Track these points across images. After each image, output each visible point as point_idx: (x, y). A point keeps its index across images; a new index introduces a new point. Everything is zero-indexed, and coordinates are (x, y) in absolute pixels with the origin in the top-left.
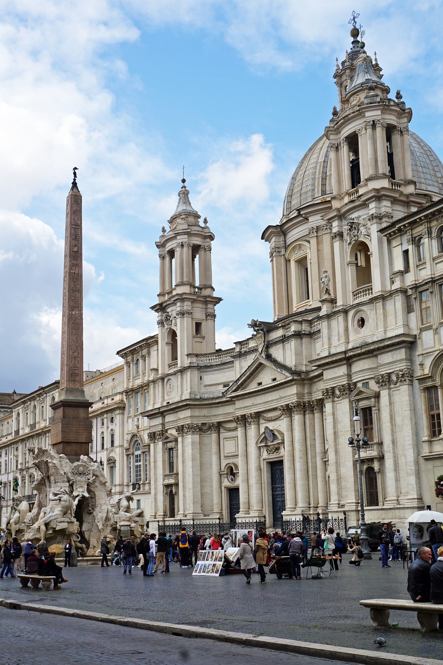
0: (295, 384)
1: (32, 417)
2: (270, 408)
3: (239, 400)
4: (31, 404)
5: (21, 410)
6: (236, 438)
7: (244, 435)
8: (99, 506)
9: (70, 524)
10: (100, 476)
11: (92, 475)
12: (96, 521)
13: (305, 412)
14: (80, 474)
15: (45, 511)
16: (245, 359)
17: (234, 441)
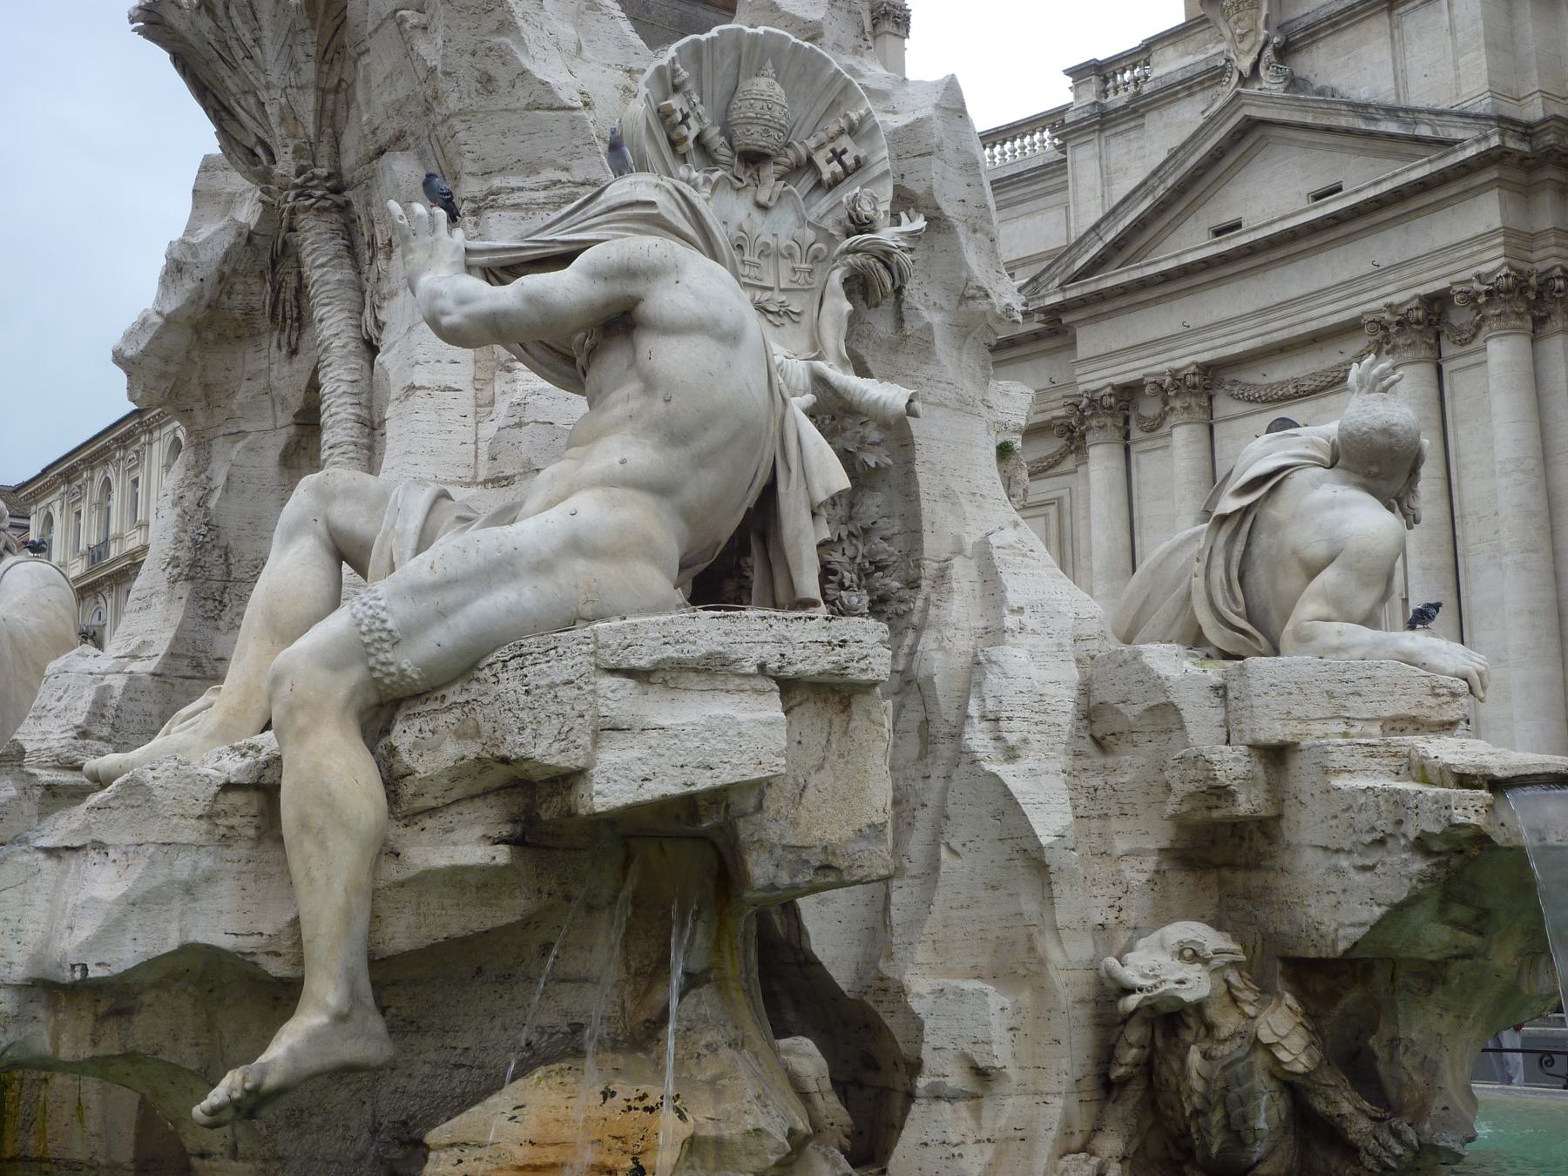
0: (1499, 182)
1: (95, 522)
2: (1300, 330)
3: (1095, 319)
4: (92, 479)
5: (58, 505)
6: (1052, 510)
7: (1121, 475)
8: (963, 573)
9: (813, 721)
10: (961, 229)
11: (886, 192)
12: (978, 738)
13: (1539, 322)
14: (753, 159)
15: (348, 516)
16: (1133, 135)
17: (1041, 520)
